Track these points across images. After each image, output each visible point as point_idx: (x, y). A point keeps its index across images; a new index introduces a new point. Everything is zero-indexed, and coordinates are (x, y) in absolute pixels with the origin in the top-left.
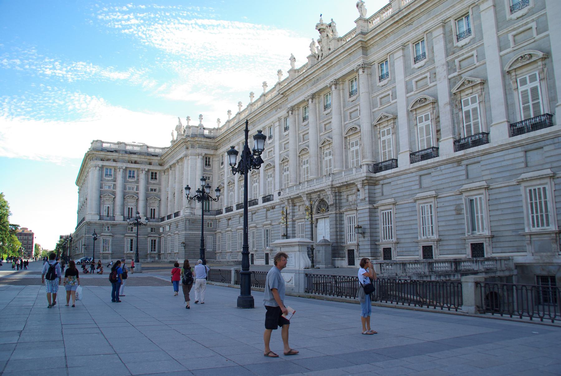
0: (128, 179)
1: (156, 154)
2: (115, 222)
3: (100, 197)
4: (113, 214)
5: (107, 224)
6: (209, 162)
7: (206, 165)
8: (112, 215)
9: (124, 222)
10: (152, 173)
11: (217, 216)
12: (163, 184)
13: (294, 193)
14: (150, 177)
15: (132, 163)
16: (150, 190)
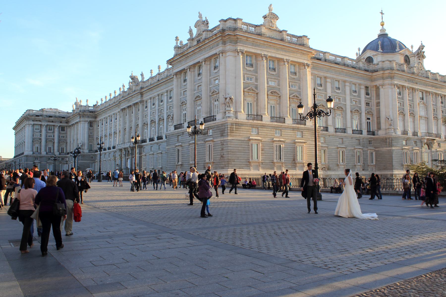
0: (48, 131)
1: (64, 116)
2: (41, 155)
3: (33, 141)
4: (40, 151)
5: (37, 156)
6: (92, 124)
7: (90, 126)
8: (39, 151)
9: (46, 155)
10: (62, 127)
11: (96, 153)
12: (68, 133)
13: (120, 148)
14: (61, 129)
15: (50, 122)
16: (61, 137)
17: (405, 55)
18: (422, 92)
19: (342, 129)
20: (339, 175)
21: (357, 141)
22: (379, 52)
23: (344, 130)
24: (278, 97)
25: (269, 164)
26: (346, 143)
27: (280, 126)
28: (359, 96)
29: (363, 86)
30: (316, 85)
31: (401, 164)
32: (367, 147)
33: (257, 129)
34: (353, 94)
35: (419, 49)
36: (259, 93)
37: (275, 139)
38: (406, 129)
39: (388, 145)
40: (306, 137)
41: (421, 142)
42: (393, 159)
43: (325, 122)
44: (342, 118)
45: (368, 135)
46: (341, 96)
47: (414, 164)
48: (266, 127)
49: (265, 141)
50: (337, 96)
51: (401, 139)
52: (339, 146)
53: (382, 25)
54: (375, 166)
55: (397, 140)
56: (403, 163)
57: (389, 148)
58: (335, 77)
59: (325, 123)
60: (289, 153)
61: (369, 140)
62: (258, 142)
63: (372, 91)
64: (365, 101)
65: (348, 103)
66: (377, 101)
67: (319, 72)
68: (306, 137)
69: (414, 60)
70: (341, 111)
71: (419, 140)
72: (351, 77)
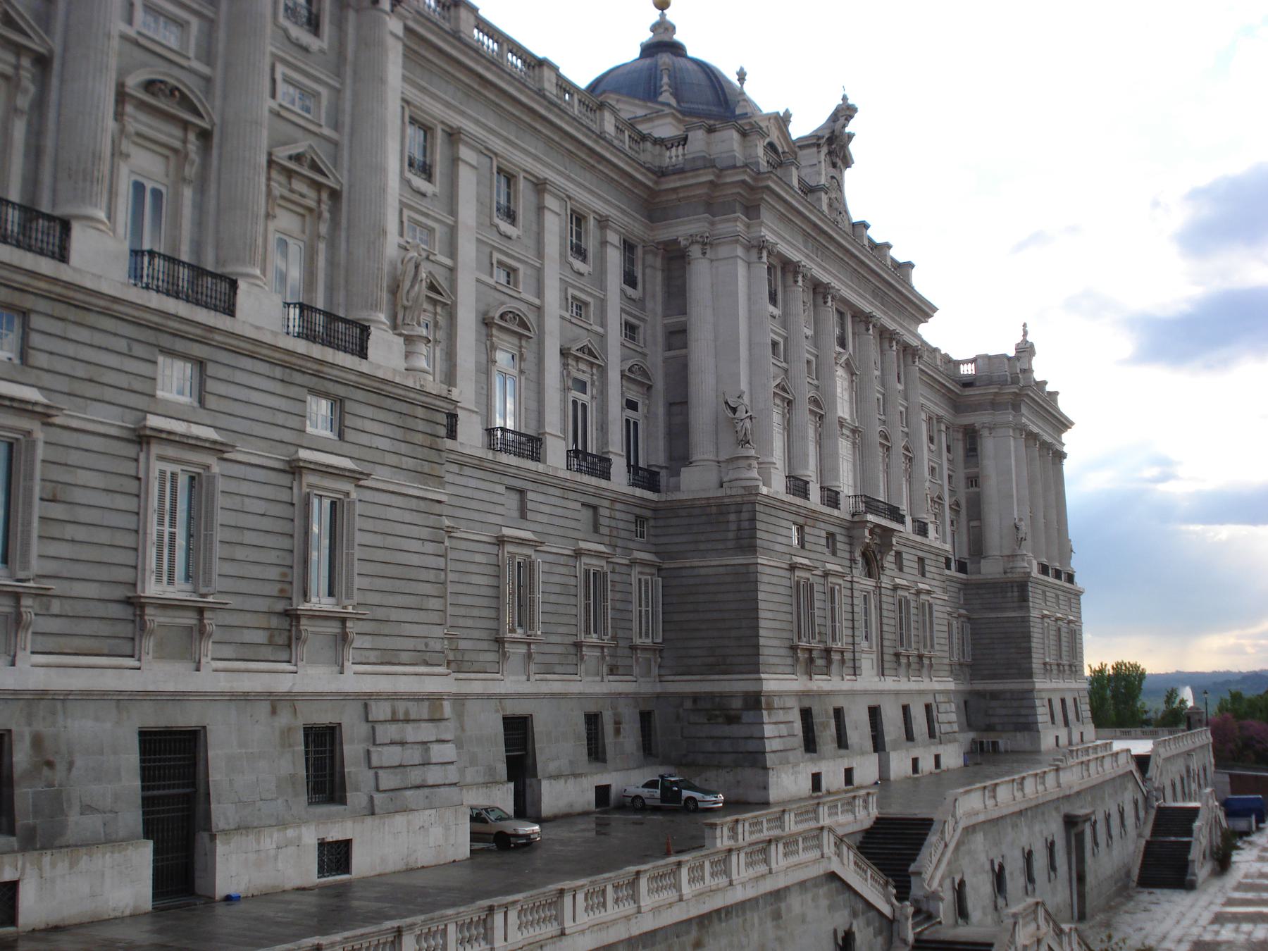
17: (768, 140)
18: (841, 314)
19: (520, 434)
20: (501, 698)
21: (587, 514)
22: (663, 104)
23: (531, 445)
24: (192, 137)
25: (101, 610)
26: (539, 518)
27: (199, 332)
29: (616, 231)
31: (787, 644)
33: (17, 322)
35: (835, 117)
36: (56, 65)
37: (153, 421)
38: (799, 472)
39: (730, 544)
40: (364, 439)
41: (851, 540)
42: (762, 614)
45: (634, 485)
47: (830, 644)
48: (91, 319)
49: (74, 424)
50: (500, 251)
51: (785, 515)
52: (507, 531)
54: (658, 650)
55: (772, 520)
56: (796, 640)
57: (740, 560)
58: (497, 145)
60: (249, 537)
61: (638, 511)
62: (25, 423)
63: (648, 271)
64: (622, 310)
66: (668, 321)
68: (364, 439)
69: (815, 161)
70: (516, 341)
71: (843, 531)
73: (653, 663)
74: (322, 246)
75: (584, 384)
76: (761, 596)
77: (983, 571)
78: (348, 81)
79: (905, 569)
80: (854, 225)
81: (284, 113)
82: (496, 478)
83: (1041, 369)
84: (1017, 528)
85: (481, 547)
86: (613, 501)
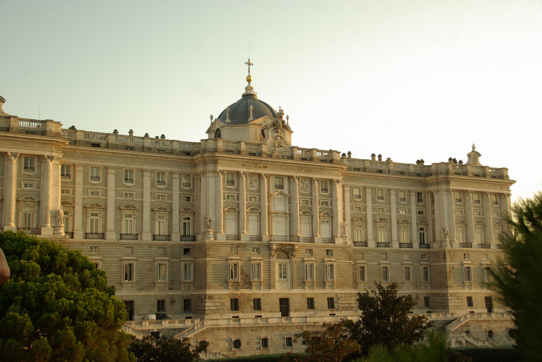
26: (138, 253)
28: (170, 188)
30: (88, 178)
31: (225, 281)
32: (179, 258)
34: (158, 186)
43: (103, 226)
44: (135, 220)
46: (134, 191)
52: (124, 258)
53: (249, 80)
54: (194, 283)
56: (229, 279)
59: (102, 228)
61: (185, 247)
63: (195, 181)
65: (147, 198)
67: (93, 161)
70: (132, 211)
71: (267, 247)
72: (154, 163)
73: (191, 287)
74: (35, 213)
75: (164, 216)
76: (207, 269)
77: (434, 247)
78: (42, 178)
79: (313, 254)
80: (292, 147)
81: (24, 190)
82: (121, 246)
83: (483, 161)
84: (444, 230)
85: (115, 262)
86: (172, 246)
